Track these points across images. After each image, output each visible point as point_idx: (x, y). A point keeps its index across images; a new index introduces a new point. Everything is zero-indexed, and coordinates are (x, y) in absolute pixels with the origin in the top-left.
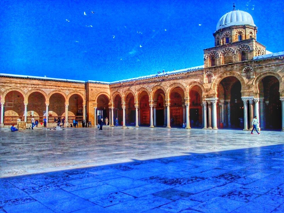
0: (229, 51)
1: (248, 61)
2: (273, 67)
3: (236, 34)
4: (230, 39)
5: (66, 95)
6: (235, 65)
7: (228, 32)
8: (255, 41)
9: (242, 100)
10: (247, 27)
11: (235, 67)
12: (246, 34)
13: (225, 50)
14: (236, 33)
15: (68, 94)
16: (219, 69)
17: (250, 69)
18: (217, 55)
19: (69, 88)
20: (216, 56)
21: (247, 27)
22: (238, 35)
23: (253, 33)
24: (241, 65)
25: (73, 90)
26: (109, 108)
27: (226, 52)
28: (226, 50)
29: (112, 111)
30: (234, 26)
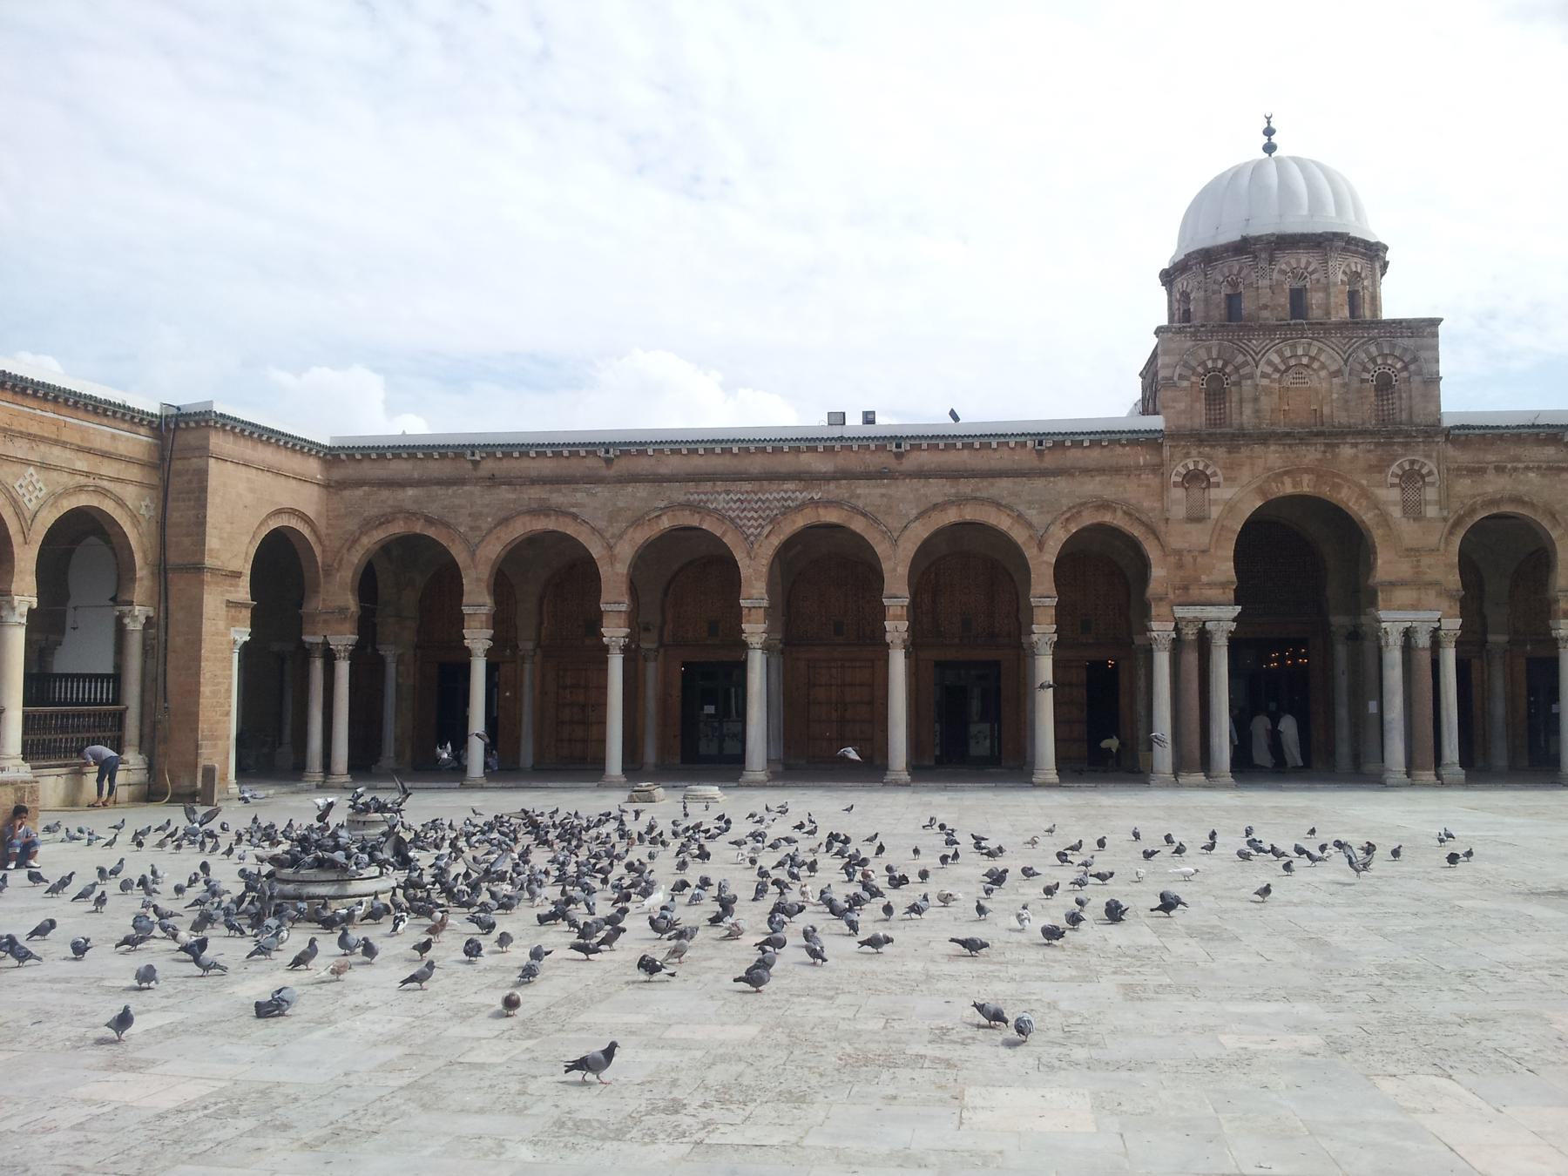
0: (1313, 359)
4: (1315, 299)
5: (19, 514)
6: (1349, 440)
7: (1308, 263)
9: (1384, 625)
11: (1346, 451)
13: (1288, 353)
14: (1340, 276)
15: (32, 506)
17: (1424, 471)
18: (1242, 372)
19: (43, 448)
20: (1234, 378)
24: (1378, 444)
25: (74, 472)
26: (307, 638)
27: (1293, 362)
28: (1294, 356)
29: (343, 669)
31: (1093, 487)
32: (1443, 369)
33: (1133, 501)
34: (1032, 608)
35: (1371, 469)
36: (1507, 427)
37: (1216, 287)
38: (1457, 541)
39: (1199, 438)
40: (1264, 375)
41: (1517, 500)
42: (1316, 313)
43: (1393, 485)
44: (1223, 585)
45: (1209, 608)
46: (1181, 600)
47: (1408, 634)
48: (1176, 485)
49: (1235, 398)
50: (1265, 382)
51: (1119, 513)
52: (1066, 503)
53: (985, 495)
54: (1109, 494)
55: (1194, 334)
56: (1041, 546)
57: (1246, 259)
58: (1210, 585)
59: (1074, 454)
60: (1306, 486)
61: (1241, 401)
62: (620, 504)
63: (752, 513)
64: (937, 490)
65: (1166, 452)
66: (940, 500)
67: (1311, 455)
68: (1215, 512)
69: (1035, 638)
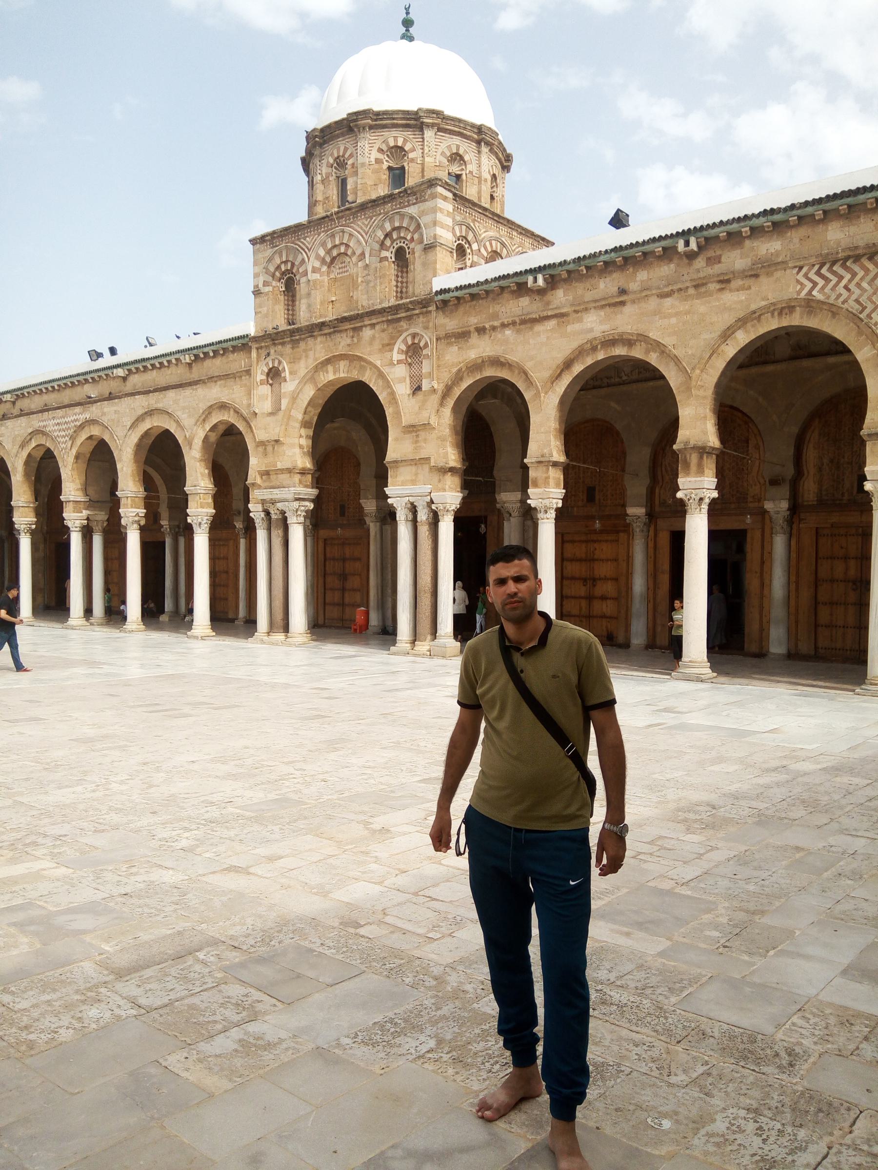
1: (411, 302)
2: (508, 332)
3: (378, 161)
7: (346, 149)
8: (450, 195)
10: (429, 126)
11: (367, 333)
12: (427, 159)
14: (375, 154)
16: (310, 341)
21: (433, 125)
22: (385, 165)
23: (466, 158)
27: (335, 253)
30: (365, 113)
33: (237, 400)
36: (478, 284)
43: (399, 362)
45: (276, 491)
46: (266, 484)
50: (317, 276)
51: (232, 412)
52: (203, 406)
53: (160, 405)
56: (190, 444)
59: (208, 363)
62: (16, 433)
63: (64, 433)
64: (140, 404)
65: (254, 354)
66: (140, 412)
67: (342, 343)
68: (284, 403)
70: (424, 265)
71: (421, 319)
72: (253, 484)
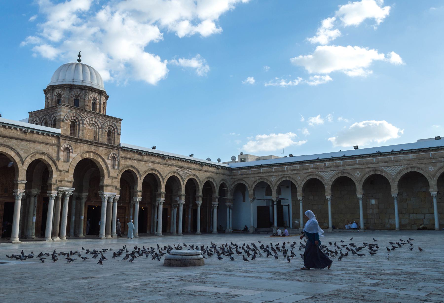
4: (98, 106)
11: (101, 149)
13: (91, 120)
27: (91, 122)
28: (92, 121)
30: (105, 92)
31: (40, 147)
32: (122, 132)
33: (50, 154)
34: (18, 184)
35: (105, 154)
37: (72, 96)
38: (120, 175)
39: (69, 139)
40: (85, 124)
41: (132, 167)
42: (98, 111)
44: (71, 182)
45: (67, 188)
47: (109, 198)
48: (62, 151)
49: (78, 129)
50: (85, 126)
51: (46, 156)
52: (32, 151)
53: (7, 144)
54: (44, 150)
55: (70, 108)
56: (23, 163)
57: (83, 91)
58: (68, 181)
59: (36, 136)
60: (91, 156)
61: (79, 130)
67: (93, 148)
68: (71, 160)
69: (18, 193)
70: (117, 138)
71: (116, 150)
72: (55, 184)
